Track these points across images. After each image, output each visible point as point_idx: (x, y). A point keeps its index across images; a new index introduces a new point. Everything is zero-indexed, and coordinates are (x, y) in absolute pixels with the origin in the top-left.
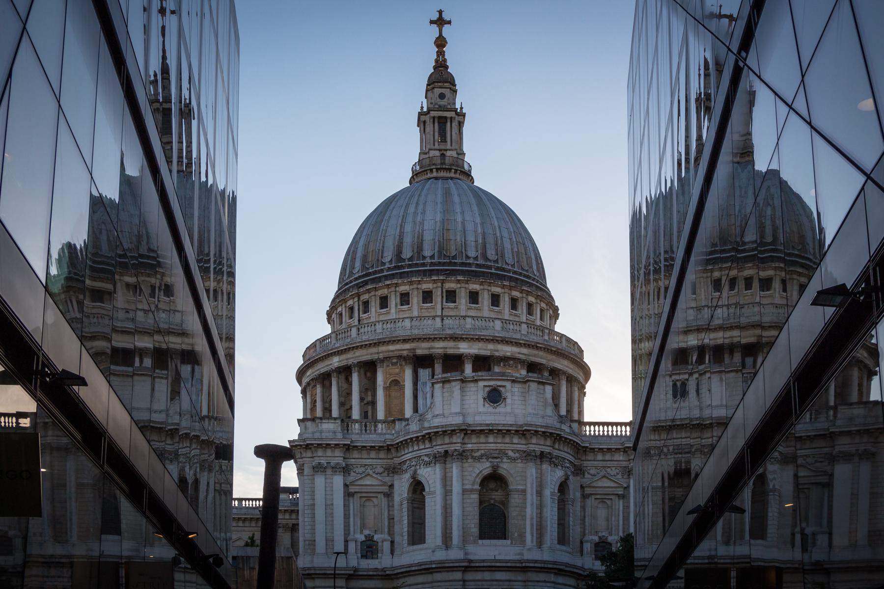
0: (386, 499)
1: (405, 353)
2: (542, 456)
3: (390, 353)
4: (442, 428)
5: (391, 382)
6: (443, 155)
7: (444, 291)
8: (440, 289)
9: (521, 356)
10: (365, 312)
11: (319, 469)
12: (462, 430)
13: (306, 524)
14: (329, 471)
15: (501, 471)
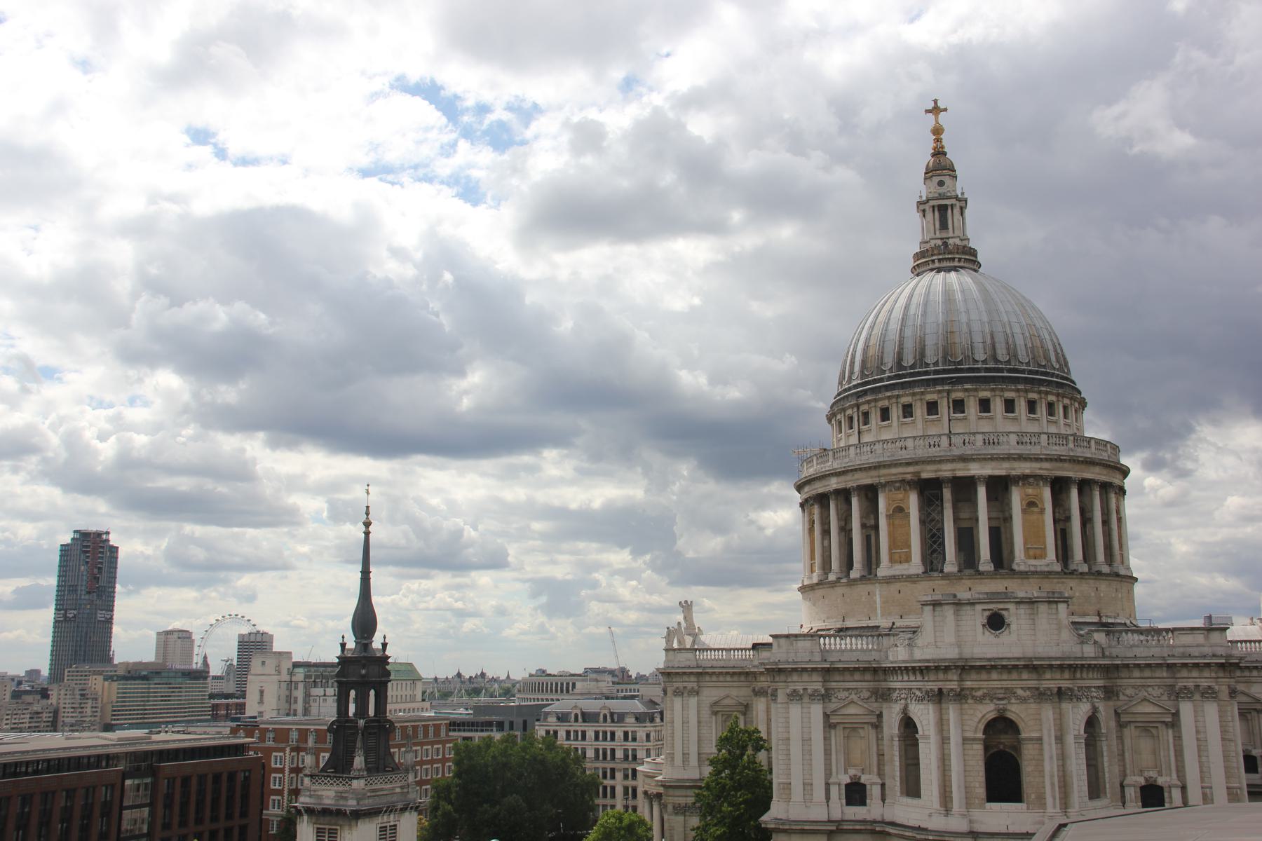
0: (874, 731)
1: (909, 477)
2: (1061, 694)
3: (893, 477)
4: (935, 662)
5: (894, 509)
6: (945, 244)
7: (951, 401)
8: (946, 400)
9: (1042, 472)
10: (865, 423)
11: (795, 696)
12: (956, 667)
13: (781, 762)
14: (806, 699)
15: (1009, 715)
